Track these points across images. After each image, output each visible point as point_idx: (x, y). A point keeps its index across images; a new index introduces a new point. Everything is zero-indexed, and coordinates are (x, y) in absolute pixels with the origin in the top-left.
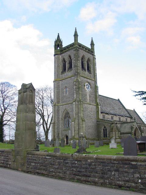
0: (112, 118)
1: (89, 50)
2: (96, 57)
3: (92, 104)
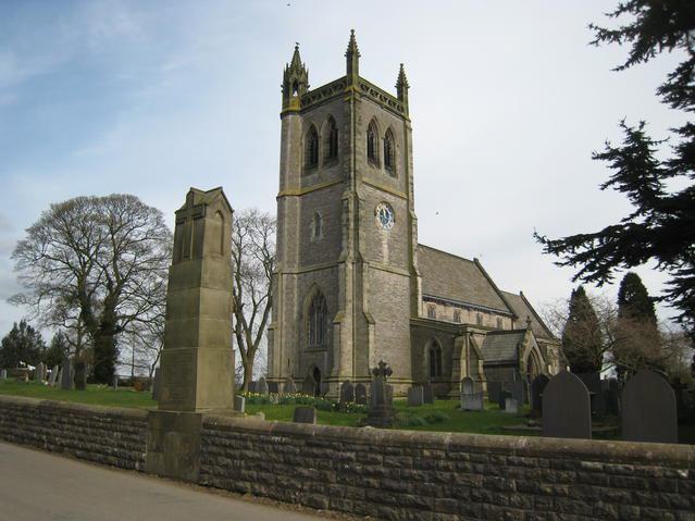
0: (457, 316)
1: (392, 101)
2: (412, 125)
3: (395, 270)
